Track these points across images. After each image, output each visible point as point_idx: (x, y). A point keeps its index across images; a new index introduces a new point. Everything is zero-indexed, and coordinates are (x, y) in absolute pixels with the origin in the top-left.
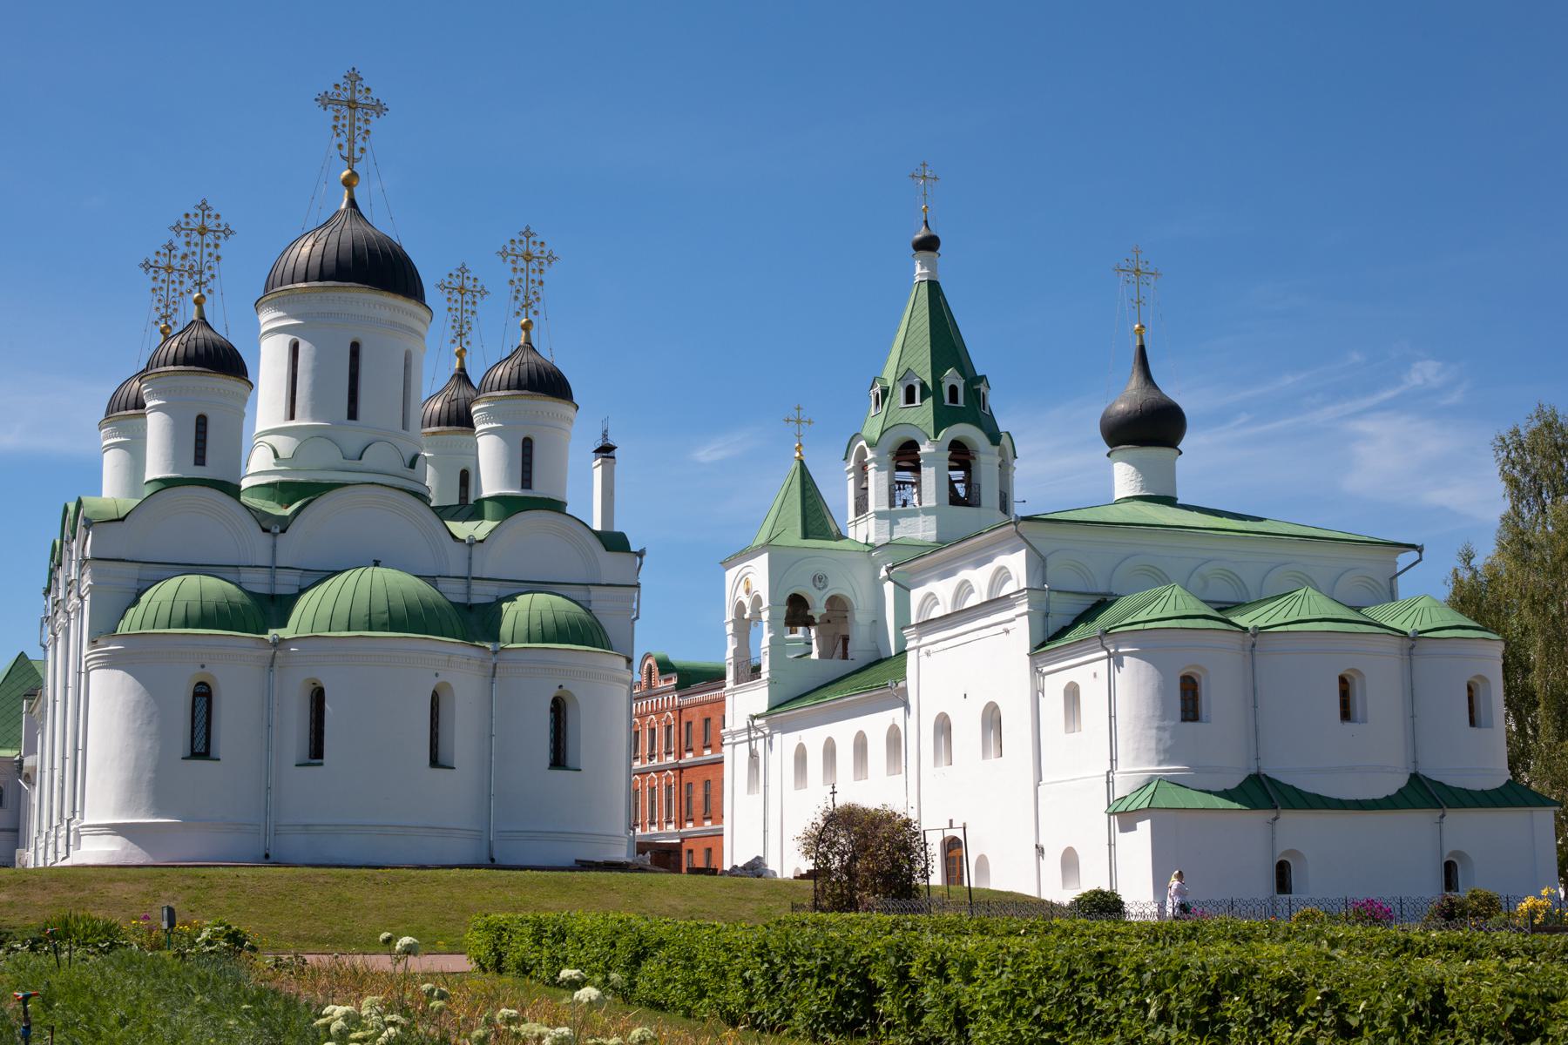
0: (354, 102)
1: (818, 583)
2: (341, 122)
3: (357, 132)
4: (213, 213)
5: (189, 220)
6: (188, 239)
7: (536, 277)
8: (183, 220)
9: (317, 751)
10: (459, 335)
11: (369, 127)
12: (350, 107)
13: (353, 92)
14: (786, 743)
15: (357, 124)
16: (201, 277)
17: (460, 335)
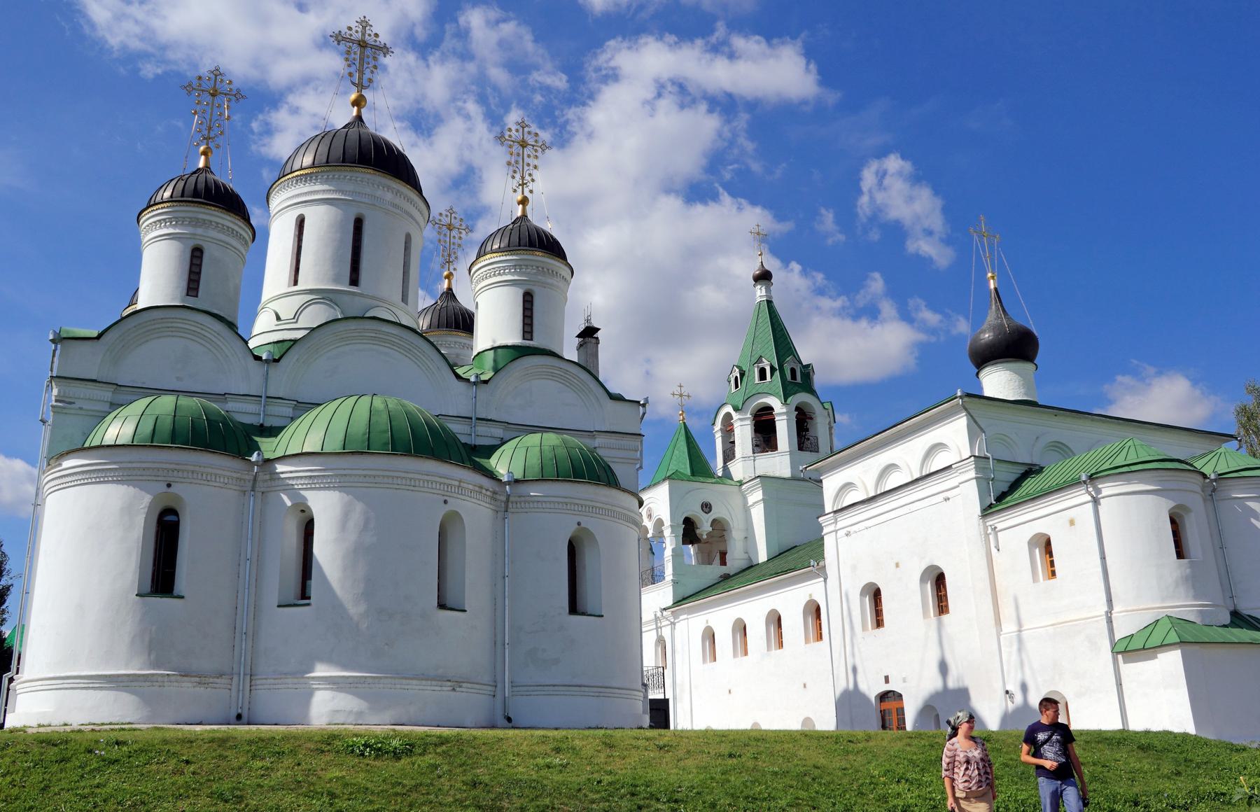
0: (364, 42)
1: (704, 508)
3: (365, 66)
7: (531, 161)
13: (363, 34)
14: (692, 625)
15: (366, 59)
16: (209, 132)
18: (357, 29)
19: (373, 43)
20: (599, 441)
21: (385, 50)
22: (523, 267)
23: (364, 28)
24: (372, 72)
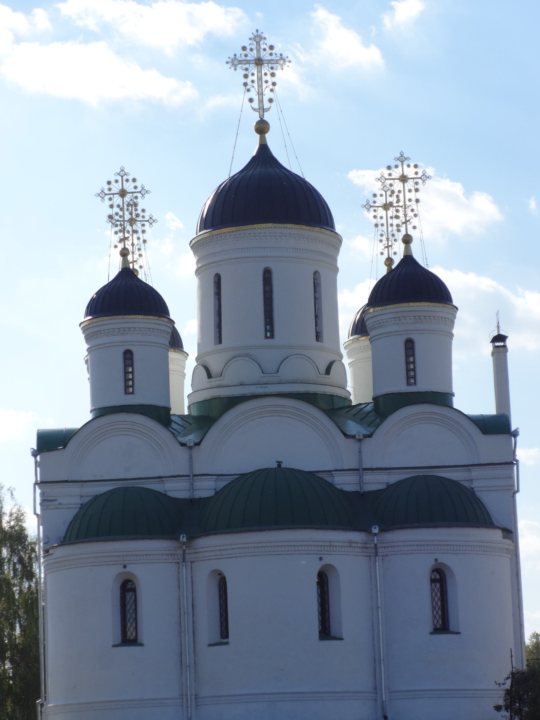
2: (251, 78)
3: (265, 86)
4: (130, 178)
5: (111, 186)
6: (111, 202)
8: (106, 187)
9: (224, 632)
10: (386, 247)
11: (274, 79)
12: (257, 64)
13: (258, 51)
15: (264, 78)
17: (388, 247)
18: (251, 46)
19: (269, 58)
20: (476, 473)
21: (281, 62)
22: (401, 318)
23: (258, 43)
24: (272, 90)
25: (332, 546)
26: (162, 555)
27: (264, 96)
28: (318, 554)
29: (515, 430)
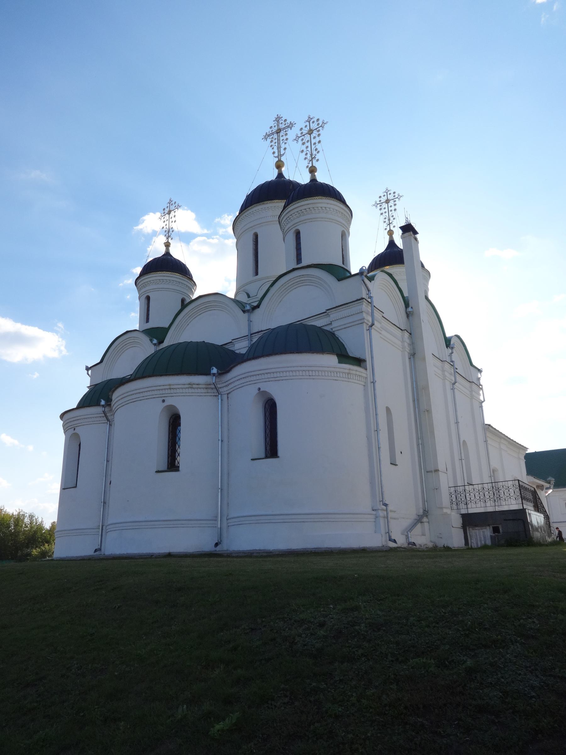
3: (281, 142)
10: (388, 225)
15: (281, 138)
17: (389, 224)
18: (274, 125)
20: (334, 315)
23: (278, 121)
25: (172, 388)
26: (96, 417)
27: (281, 148)
28: (162, 397)
29: (361, 269)
